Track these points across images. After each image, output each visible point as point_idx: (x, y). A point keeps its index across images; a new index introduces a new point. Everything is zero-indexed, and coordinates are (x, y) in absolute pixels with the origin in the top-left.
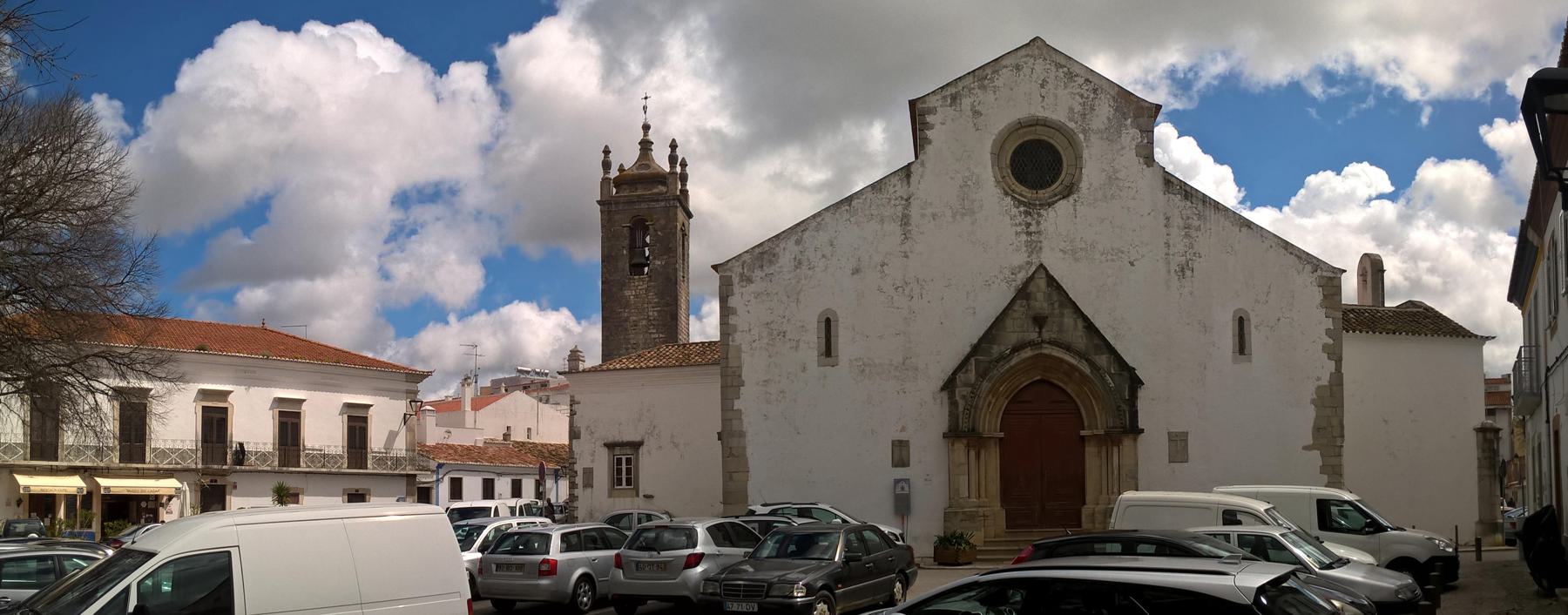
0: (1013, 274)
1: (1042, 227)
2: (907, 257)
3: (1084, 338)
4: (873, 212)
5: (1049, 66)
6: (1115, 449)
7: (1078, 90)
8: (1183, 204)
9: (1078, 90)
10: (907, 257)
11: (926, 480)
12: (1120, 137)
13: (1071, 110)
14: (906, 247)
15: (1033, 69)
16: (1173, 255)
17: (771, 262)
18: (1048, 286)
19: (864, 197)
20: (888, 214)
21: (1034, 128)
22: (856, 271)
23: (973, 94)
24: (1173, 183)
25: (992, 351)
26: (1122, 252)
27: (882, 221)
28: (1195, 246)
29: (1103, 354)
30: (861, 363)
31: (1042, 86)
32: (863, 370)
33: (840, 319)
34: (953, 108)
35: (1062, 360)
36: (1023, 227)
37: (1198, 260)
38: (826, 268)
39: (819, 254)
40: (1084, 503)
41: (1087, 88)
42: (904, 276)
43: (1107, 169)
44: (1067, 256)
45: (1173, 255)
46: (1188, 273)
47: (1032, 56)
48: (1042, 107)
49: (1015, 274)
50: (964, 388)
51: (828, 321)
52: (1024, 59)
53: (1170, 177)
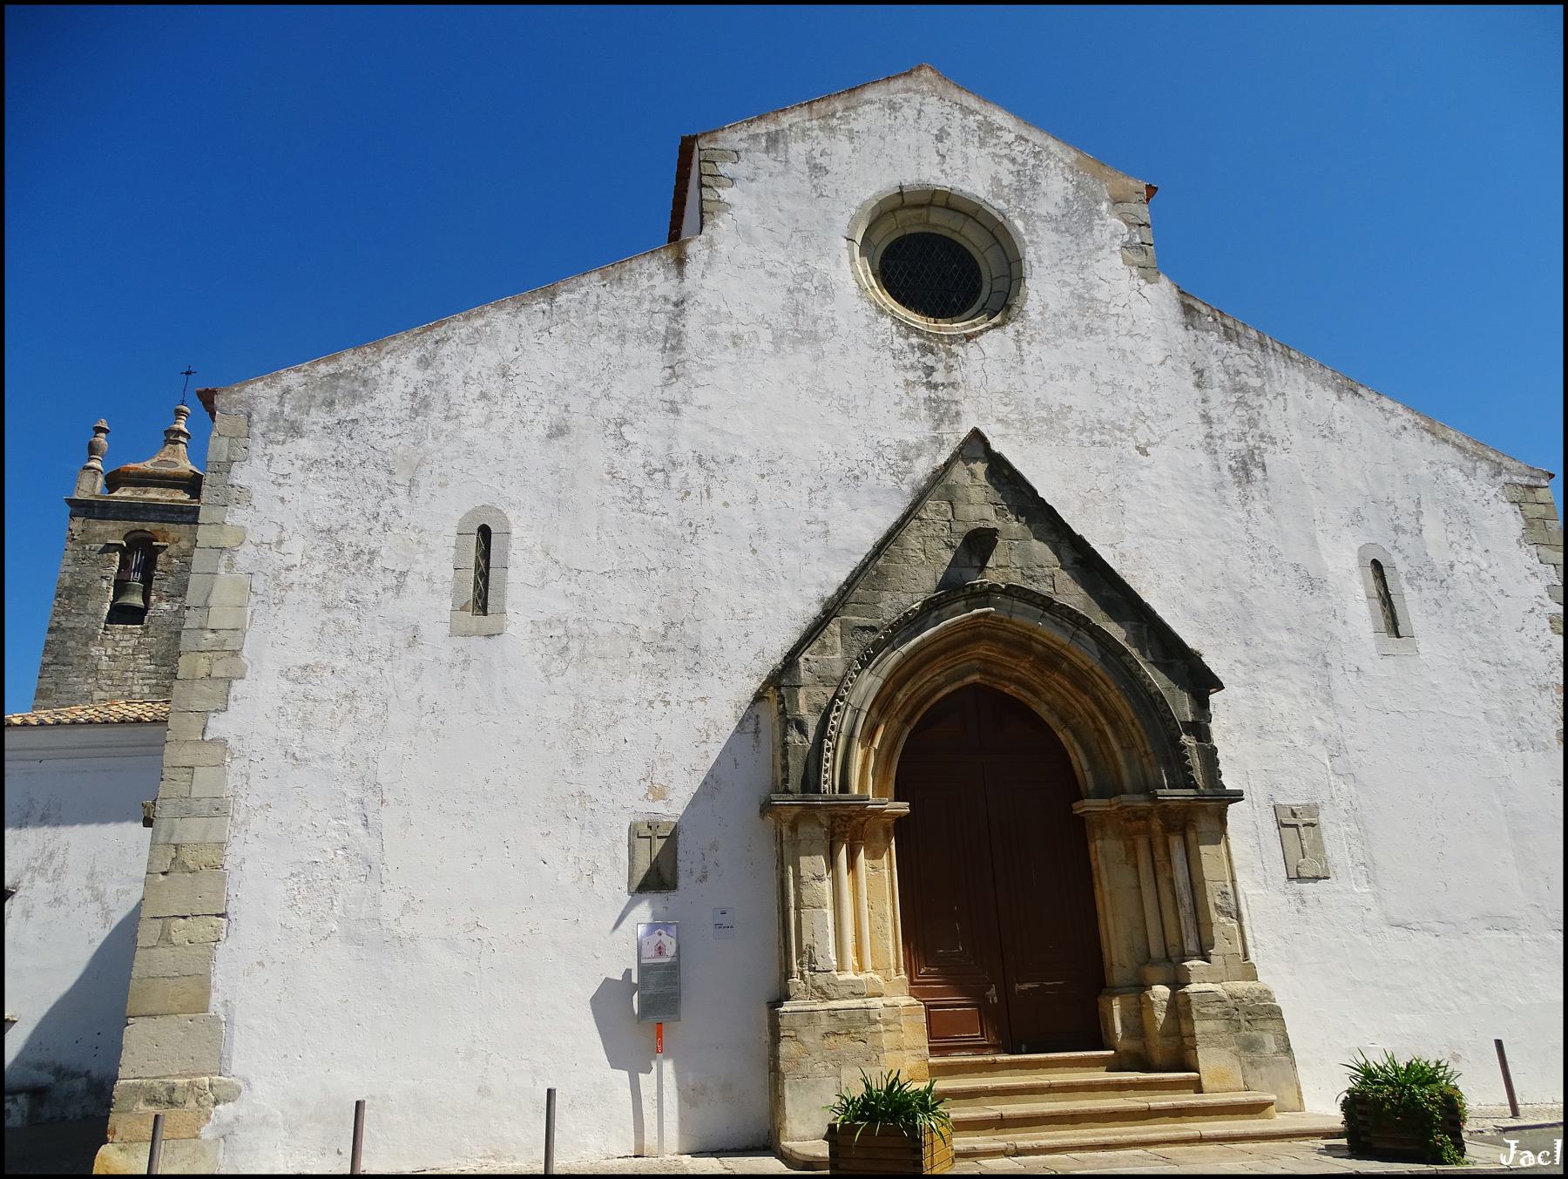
0: (904, 459)
4: (602, 319)
5: (948, 110)
6: (1176, 842)
7: (1007, 151)
8: (1224, 347)
9: (1007, 151)
12: (1091, 230)
13: (996, 180)
14: (675, 392)
15: (920, 111)
16: (1220, 438)
17: (354, 396)
19: (583, 290)
20: (635, 326)
21: (924, 211)
22: (558, 431)
23: (810, 137)
24: (1199, 312)
25: (881, 605)
27: (622, 337)
28: (1262, 425)
30: (560, 631)
31: (939, 138)
32: (566, 648)
33: (515, 532)
34: (773, 155)
36: (920, 373)
37: (1270, 447)
38: (489, 419)
39: (474, 390)
41: (1021, 149)
42: (670, 447)
43: (1073, 282)
44: (1011, 431)
45: (1220, 438)
46: (1257, 473)
47: (916, 92)
48: (942, 171)
49: (911, 461)
51: (485, 533)
52: (903, 95)
53: (1191, 302)
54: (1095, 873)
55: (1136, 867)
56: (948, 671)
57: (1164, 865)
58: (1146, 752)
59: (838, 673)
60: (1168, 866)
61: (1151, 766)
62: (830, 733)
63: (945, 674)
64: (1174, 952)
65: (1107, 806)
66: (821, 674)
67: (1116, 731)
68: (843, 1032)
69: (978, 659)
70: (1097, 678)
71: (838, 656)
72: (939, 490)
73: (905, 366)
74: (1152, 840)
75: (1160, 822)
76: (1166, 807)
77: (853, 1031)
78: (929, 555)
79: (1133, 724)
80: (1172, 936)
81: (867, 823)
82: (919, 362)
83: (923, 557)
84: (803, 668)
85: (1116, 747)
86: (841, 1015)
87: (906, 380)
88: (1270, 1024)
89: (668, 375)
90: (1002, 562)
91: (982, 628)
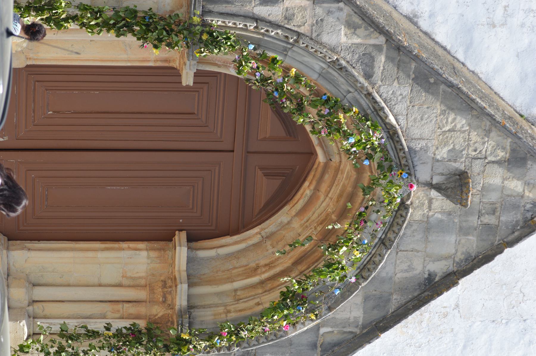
29: (365, 313)
54: (116, 245)
55: (119, 285)
57: (119, 311)
58: (229, 312)
59: (325, 38)
60: (117, 315)
61: (215, 315)
62: (262, 29)
64: (38, 308)
65: (179, 267)
67: (253, 286)
71: (343, 39)
74: (144, 304)
75: (159, 315)
78: (448, 135)
79: (258, 304)
80: (51, 309)
83: (447, 128)
85: (237, 284)
90: (436, 204)
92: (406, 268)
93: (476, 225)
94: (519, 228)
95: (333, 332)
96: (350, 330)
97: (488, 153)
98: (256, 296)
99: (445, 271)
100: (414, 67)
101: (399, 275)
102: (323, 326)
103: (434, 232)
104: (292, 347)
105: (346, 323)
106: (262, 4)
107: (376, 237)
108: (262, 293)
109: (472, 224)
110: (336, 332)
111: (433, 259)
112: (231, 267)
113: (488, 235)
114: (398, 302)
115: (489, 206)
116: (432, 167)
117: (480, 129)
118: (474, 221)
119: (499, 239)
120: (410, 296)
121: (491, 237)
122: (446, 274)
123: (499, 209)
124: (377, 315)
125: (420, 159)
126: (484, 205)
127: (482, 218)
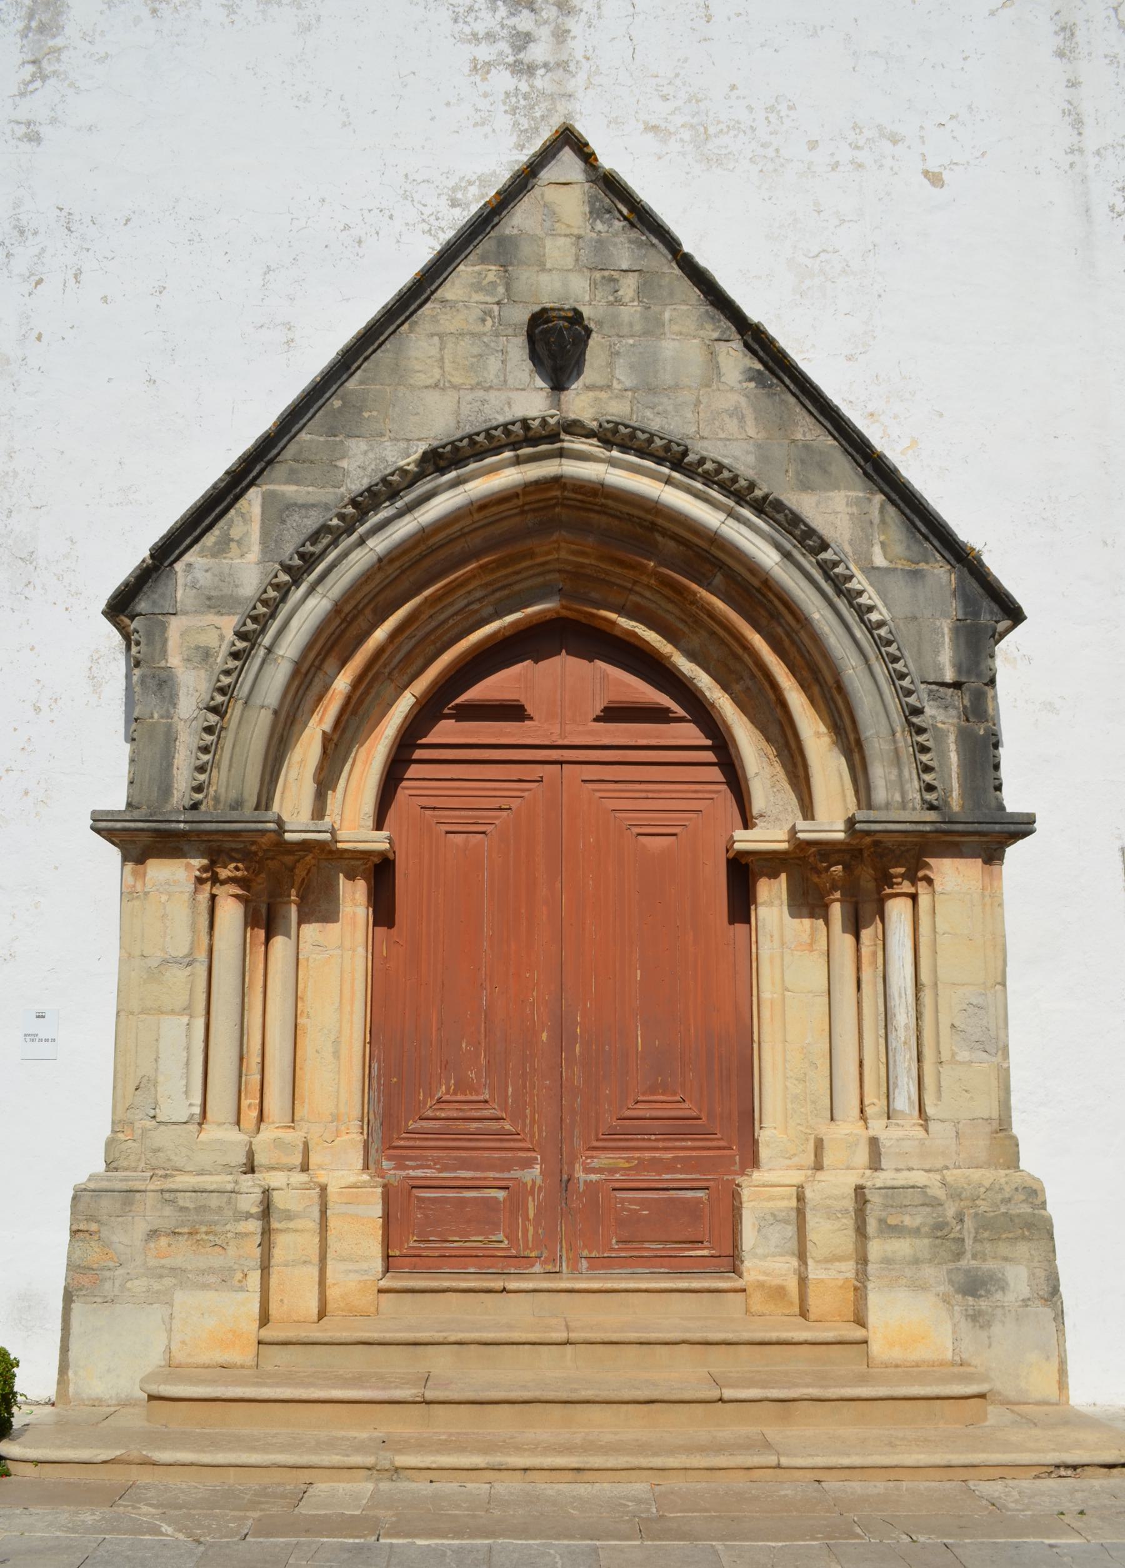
1: (577, 46)
2: (34, 138)
3: (750, 422)
6: (898, 910)
10: (34, 138)
11: (31, 1037)
18: (596, 213)
25: (344, 464)
26: (895, 140)
35: (655, 508)
36: (504, 46)
40: (752, 1160)
42: (17, 205)
50: (212, 618)
56: (498, 595)
63: (492, 598)
66: (213, 593)
68: (186, 1230)
69: (559, 571)
70: (777, 603)
72: (486, 244)
73: (475, 35)
76: (876, 843)
77: (204, 1229)
81: (299, 865)
82: (503, 26)
84: (181, 581)
86: (185, 1200)
87: (475, 60)
88: (1023, 1248)
89: (28, 78)
91: (557, 510)
92: (735, 421)
93: (639, 309)
94: (644, 238)
95: (883, 544)
96: (877, 512)
97: (489, 299)
98: (828, 696)
99: (740, 355)
100: (309, 436)
101: (751, 432)
102: (869, 558)
103: (655, 377)
104: (918, 615)
105: (862, 522)
106: (175, 704)
107: (669, 476)
108: (821, 686)
109: (638, 315)
110: (882, 538)
111: (715, 376)
112: (786, 752)
113: (660, 286)
114: (810, 430)
115: (600, 290)
116: (518, 389)
117: (439, 317)
118: (630, 312)
119: (669, 268)
120: (798, 410)
121: (665, 281)
122: (746, 351)
123: (606, 273)
124: (842, 464)
125: (501, 411)
126: (597, 298)
127: (626, 300)
